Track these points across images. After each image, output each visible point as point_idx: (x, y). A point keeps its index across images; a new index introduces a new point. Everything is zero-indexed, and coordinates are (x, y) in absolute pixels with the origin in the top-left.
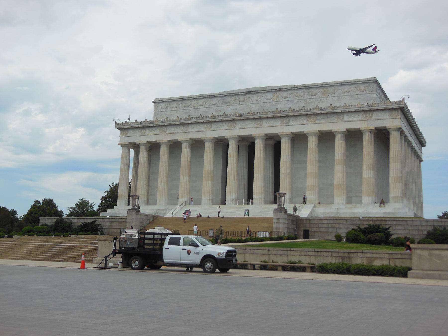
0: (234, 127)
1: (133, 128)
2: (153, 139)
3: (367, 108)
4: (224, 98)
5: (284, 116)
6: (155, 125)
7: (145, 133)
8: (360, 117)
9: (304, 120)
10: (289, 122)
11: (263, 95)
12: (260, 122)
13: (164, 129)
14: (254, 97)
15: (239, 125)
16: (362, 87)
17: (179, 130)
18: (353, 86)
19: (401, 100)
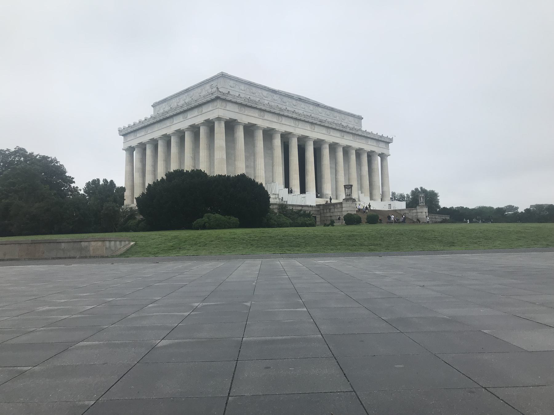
0: (314, 129)
1: (236, 103)
2: (253, 121)
3: (380, 139)
4: (282, 97)
5: (343, 131)
6: (259, 107)
7: (245, 112)
8: (374, 143)
9: (350, 137)
10: (343, 137)
11: (308, 105)
12: (329, 130)
13: (262, 113)
14: (303, 105)
15: (317, 128)
16: (357, 120)
17: (274, 119)
18: (353, 118)
19: (391, 138)
